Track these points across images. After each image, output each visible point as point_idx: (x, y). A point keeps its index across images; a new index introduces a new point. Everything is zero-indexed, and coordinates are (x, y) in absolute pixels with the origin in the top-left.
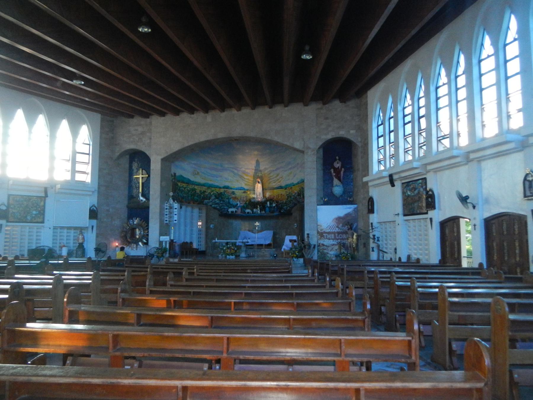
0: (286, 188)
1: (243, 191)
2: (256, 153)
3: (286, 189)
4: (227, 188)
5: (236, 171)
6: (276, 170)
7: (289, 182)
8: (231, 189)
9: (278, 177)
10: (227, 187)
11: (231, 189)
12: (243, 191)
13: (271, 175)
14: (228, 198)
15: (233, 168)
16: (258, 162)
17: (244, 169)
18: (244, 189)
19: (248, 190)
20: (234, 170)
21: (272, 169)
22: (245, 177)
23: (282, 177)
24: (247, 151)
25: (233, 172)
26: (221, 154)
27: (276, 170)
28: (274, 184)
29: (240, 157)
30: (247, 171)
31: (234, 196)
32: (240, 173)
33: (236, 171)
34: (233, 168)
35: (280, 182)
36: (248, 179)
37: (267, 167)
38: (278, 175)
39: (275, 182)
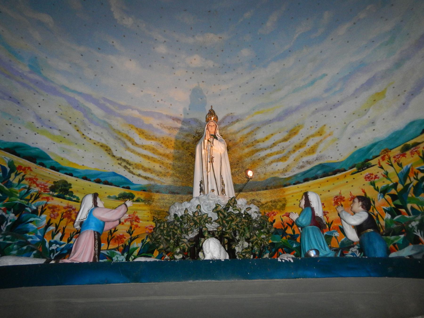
0: (361, 162)
1: (118, 191)
2: (196, 61)
3: (364, 166)
4: (32, 159)
5: (98, 112)
6: (279, 118)
7: (365, 139)
8: (56, 168)
9: (296, 140)
10: (38, 158)
11: (56, 168)
12: (118, 191)
13: (260, 136)
14: (19, 209)
15: (88, 97)
16: (197, 94)
17: (136, 114)
18: (125, 184)
19: (144, 189)
20: (91, 106)
21: (258, 118)
22: (138, 138)
23: (320, 133)
24: (162, 49)
25: (86, 112)
26: (46, 18)
27: (279, 118)
28: (281, 165)
29: (130, 66)
30: (154, 122)
31: (56, 202)
32: (117, 124)
33: (98, 112)
34: (88, 97)
35: (313, 150)
36: (154, 150)
37: (238, 112)
38: (293, 132)
39: (284, 158)
